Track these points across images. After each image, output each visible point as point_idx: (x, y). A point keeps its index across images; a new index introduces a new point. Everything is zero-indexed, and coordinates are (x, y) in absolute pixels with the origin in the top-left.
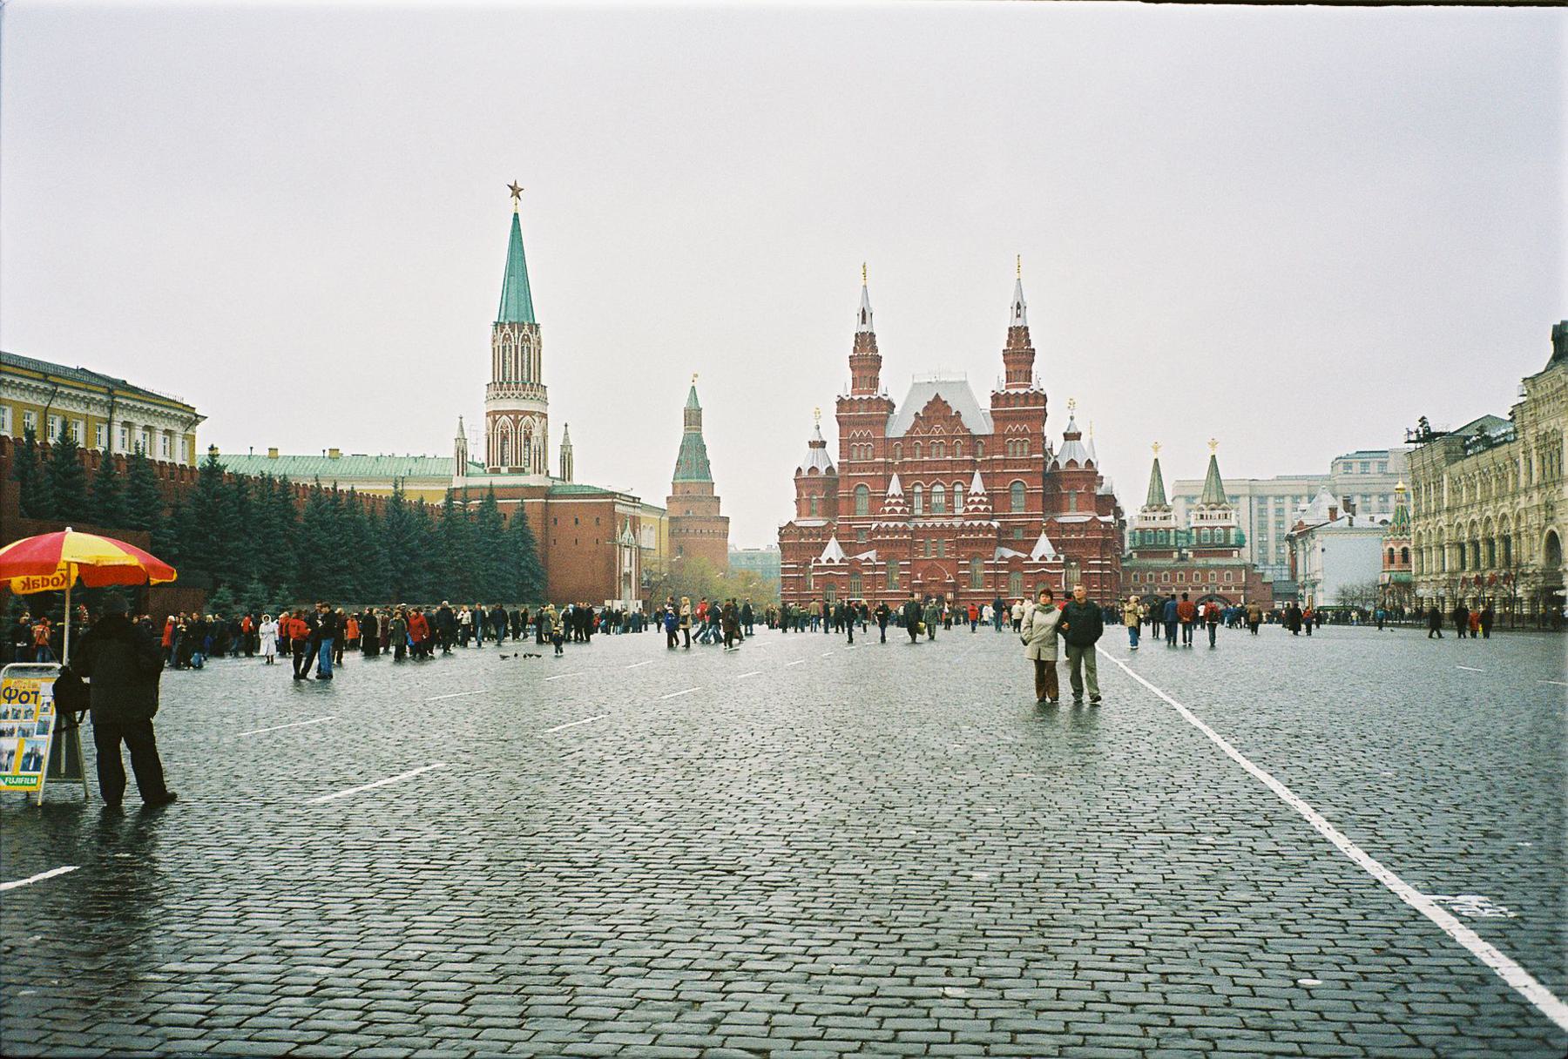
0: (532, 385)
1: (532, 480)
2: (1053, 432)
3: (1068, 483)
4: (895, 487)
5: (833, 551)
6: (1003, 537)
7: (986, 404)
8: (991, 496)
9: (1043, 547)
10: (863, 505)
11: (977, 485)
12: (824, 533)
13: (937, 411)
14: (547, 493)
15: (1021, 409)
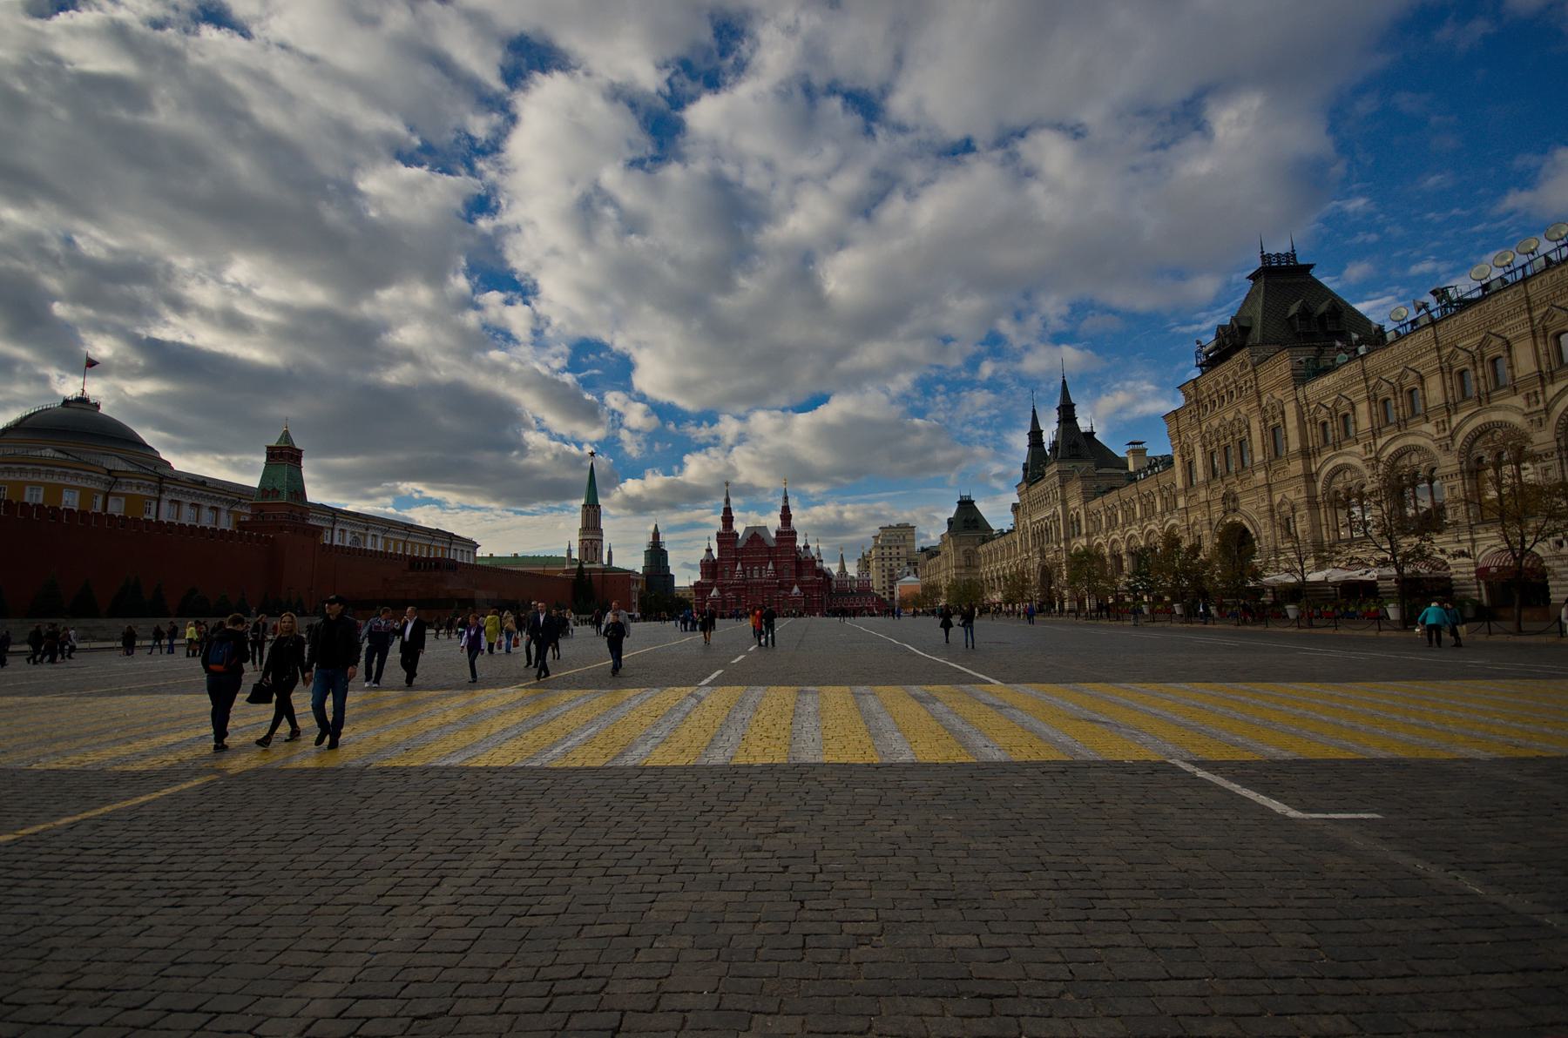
0: (599, 531)
1: (597, 566)
2: (800, 544)
3: (805, 565)
4: (739, 567)
5: (715, 592)
6: (781, 586)
7: (773, 535)
8: (776, 571)
9: (796, 589)
10: (727, 575)
11: (770, 567)
12: (711, 586)
13: (756, 535)
14: (603, 571)
15: (787, 534)
